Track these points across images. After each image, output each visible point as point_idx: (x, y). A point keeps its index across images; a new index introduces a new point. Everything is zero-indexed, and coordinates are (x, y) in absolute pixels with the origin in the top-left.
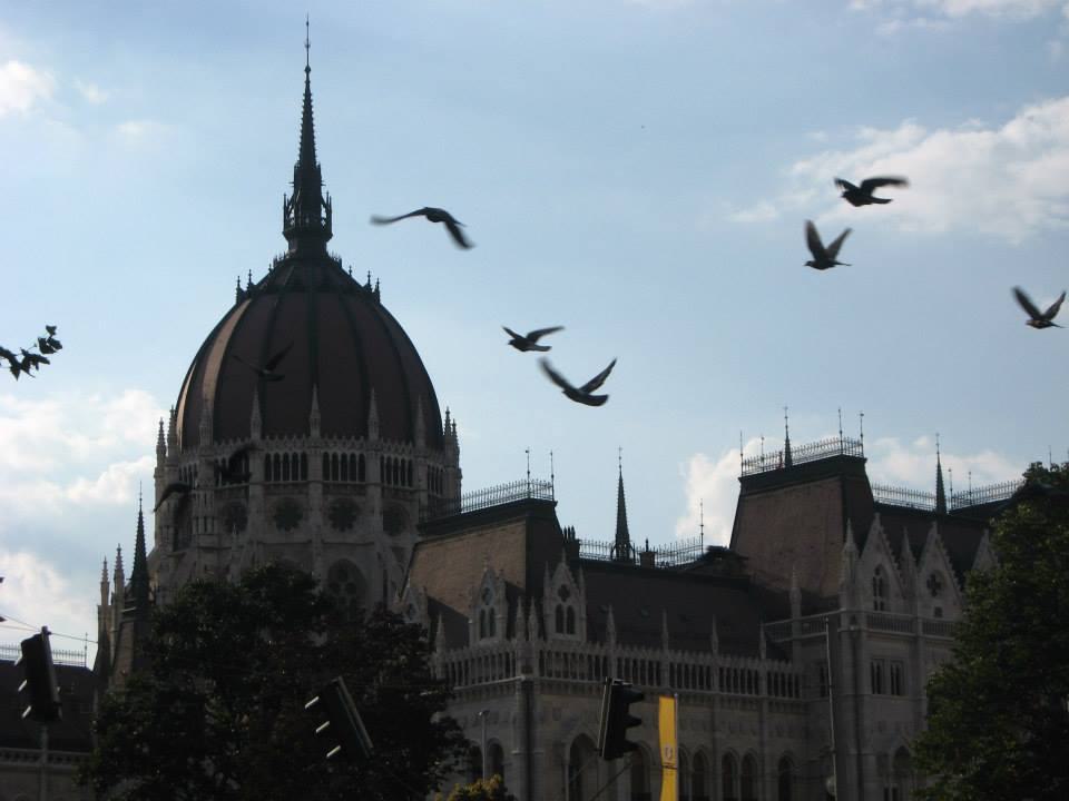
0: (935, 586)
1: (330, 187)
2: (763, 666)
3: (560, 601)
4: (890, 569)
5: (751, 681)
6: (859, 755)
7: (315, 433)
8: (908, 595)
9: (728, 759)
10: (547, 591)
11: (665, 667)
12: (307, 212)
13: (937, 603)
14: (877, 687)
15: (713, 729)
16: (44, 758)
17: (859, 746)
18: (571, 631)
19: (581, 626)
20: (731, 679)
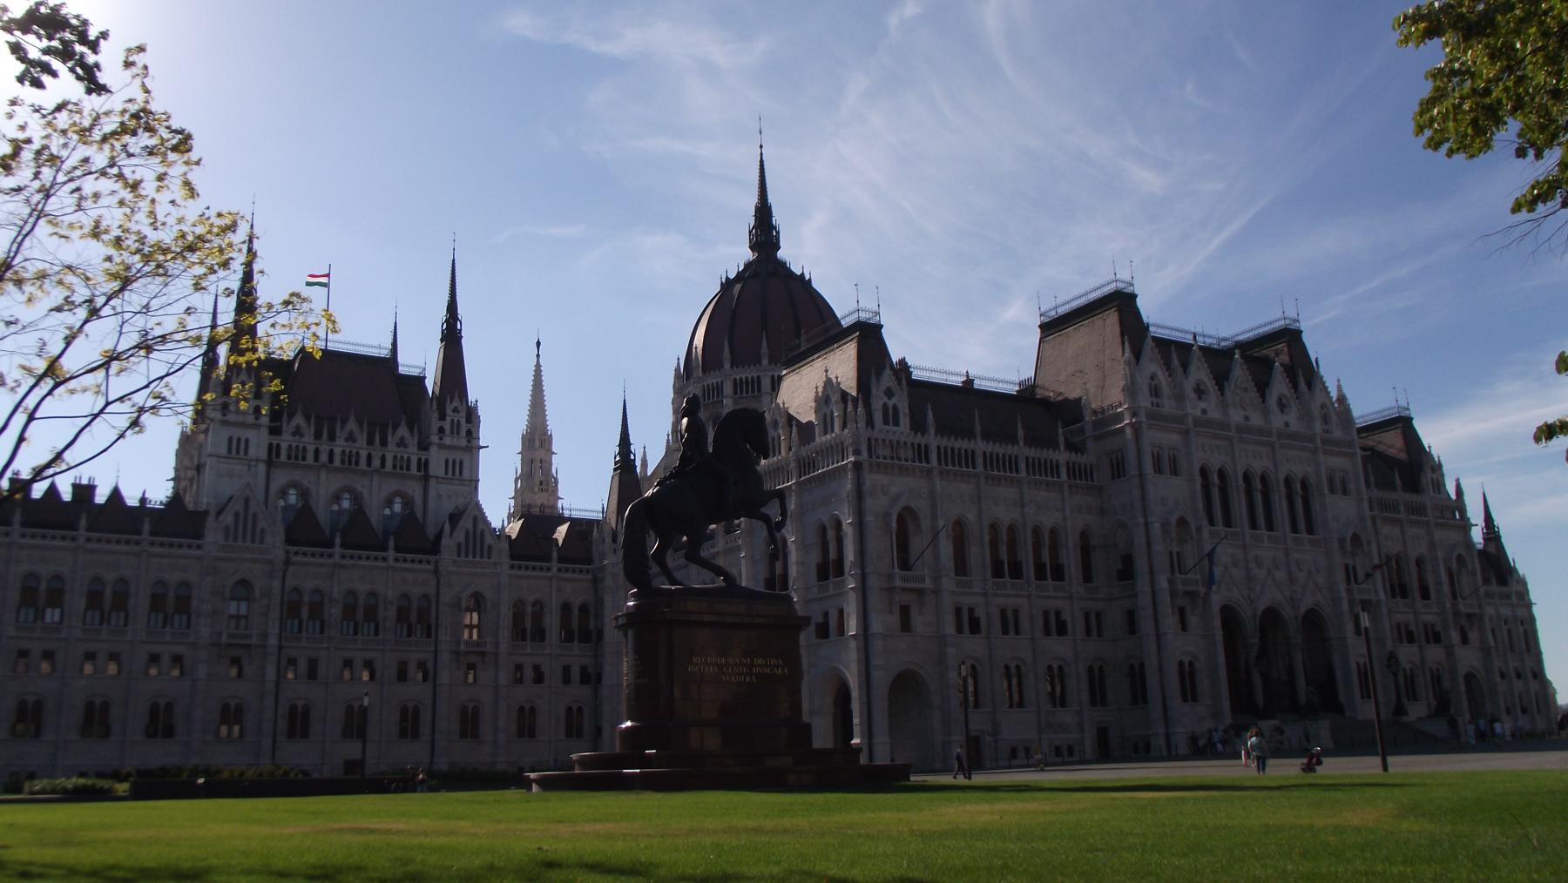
0: (1200, 392)
1: (778, 218)
2: (1062, 456)
3: (885, 399)
4: (1162, 377)
5: (1054, 468)
6: (1146, 524)
7: (765, 362)
8: (1179, 398)
9: (1036, 531)
10: (874, 390)
11: (979, 454)
12: (764, 233)
13: (1203, 405)
14: (1158, 469)
15: (1023, 506)
16: (554, 569)
17: (1145, 517)
18: (896, 423)
19: (905, 421)
20: (1035, 467)
